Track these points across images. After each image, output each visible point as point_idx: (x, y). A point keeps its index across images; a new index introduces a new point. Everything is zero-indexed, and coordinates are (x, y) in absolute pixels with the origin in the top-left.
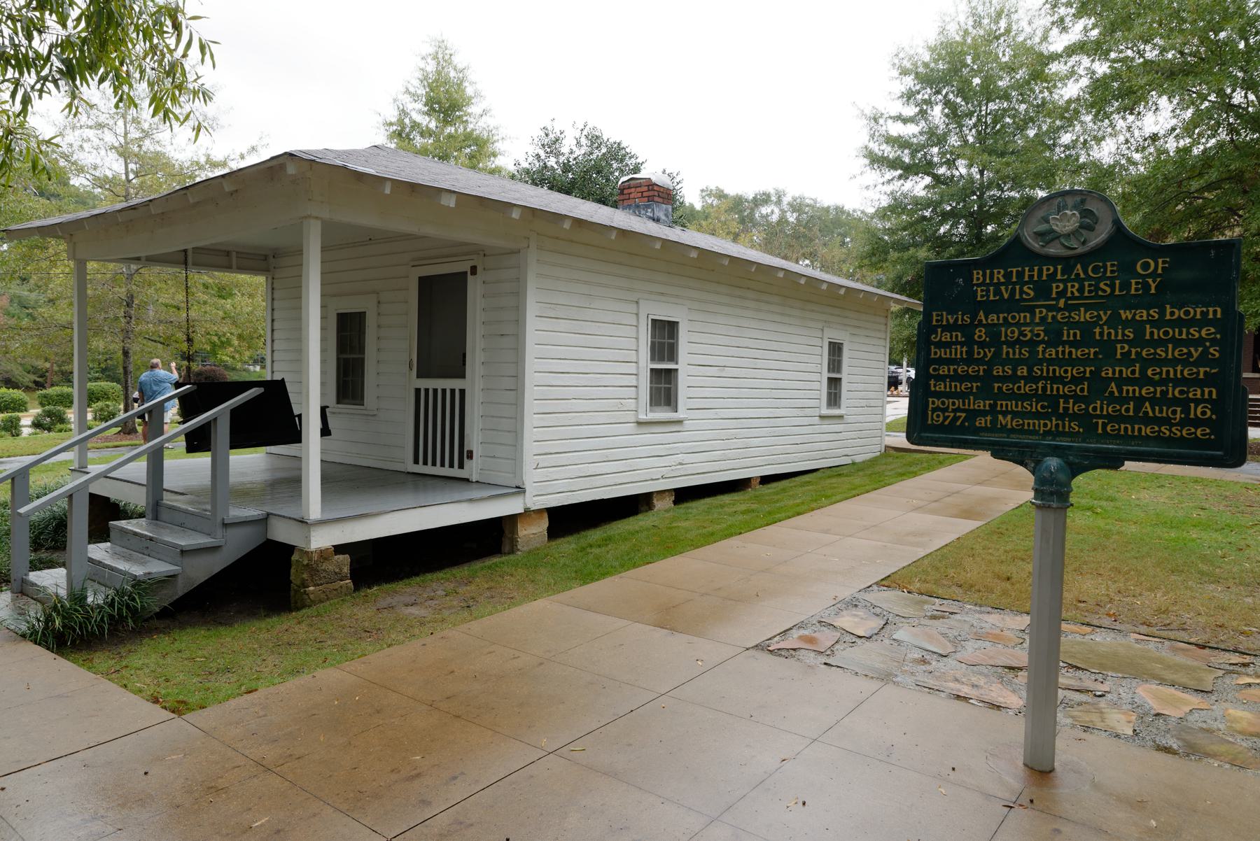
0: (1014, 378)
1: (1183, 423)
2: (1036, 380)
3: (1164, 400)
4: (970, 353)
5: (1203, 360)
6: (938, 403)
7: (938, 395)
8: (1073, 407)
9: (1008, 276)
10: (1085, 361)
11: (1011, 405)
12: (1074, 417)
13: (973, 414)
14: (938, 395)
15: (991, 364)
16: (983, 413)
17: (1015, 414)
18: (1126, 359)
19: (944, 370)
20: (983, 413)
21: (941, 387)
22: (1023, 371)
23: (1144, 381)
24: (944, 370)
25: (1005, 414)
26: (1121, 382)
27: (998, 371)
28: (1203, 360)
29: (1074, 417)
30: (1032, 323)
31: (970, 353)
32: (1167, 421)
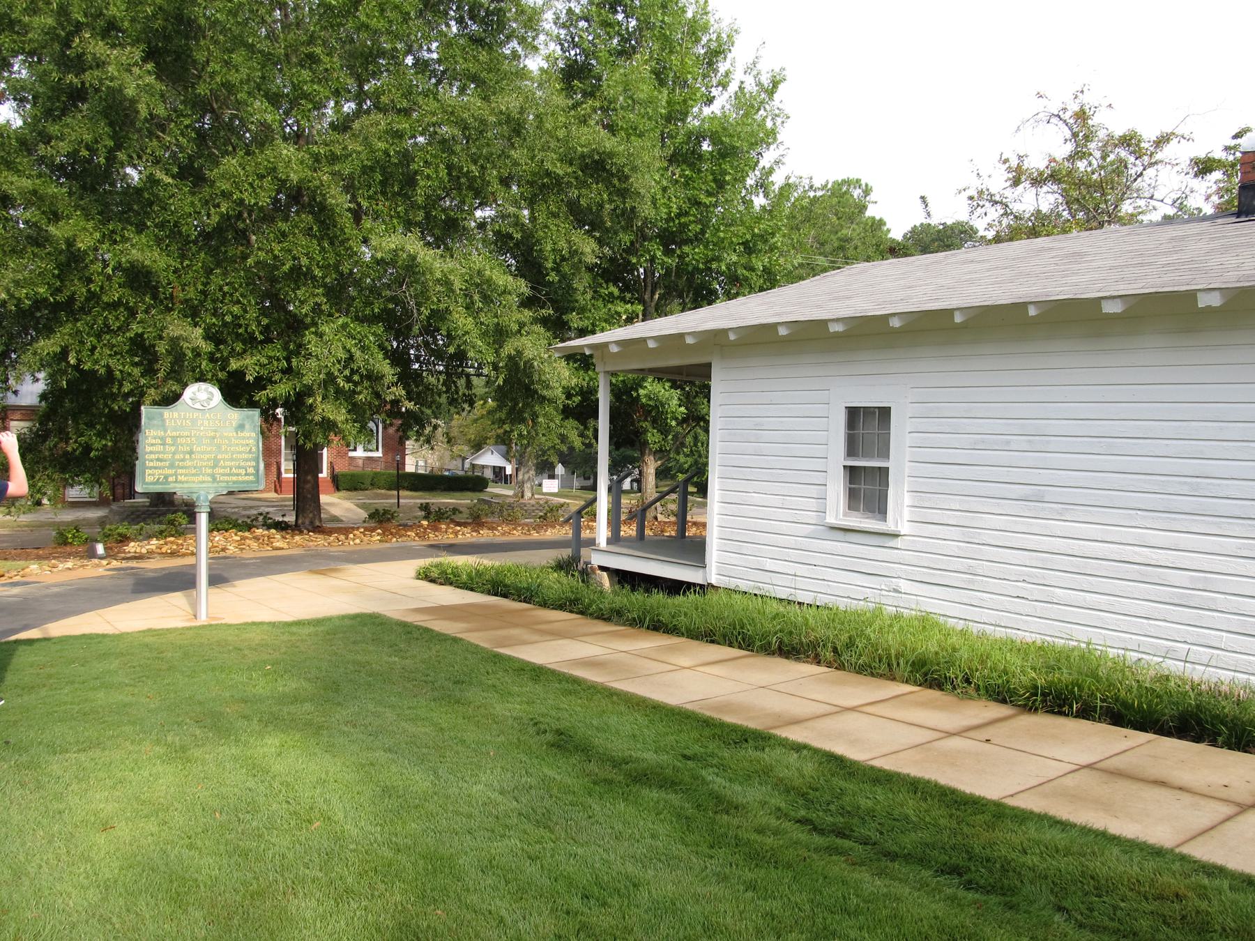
0: (182, 460)
1: (246, 474)
2: (193, 460)
3: (239, 467)
4: (164, 449)
5: (250, 452)
6: (150, 472)
7: (151, 468)
8: (209, 471)
9: (180, 415)
10: (210, 453)
11: (183, 471)
12: (208, 475)
13: (166, 477)
14: (151, 468)
15: (174, 453)
16: (172, 475)
17: (186, 475)
18: (226, 452)
19: (152, 456)
20: (172, 475)
21: (151, 464)
22: (187, 456)
23: (232, 460)
24: (152, 456)
25: (181, 475)
26: (224, 460)
27: (177, 457)
28: (250, 452)
29: (208, 475)
30: (190, 436)
31: (164, 449)
32: (238, 475)
